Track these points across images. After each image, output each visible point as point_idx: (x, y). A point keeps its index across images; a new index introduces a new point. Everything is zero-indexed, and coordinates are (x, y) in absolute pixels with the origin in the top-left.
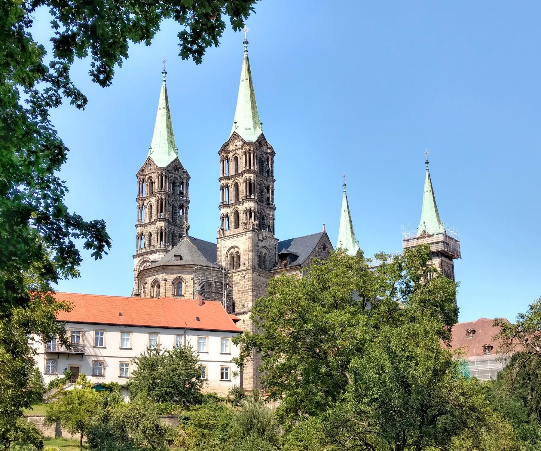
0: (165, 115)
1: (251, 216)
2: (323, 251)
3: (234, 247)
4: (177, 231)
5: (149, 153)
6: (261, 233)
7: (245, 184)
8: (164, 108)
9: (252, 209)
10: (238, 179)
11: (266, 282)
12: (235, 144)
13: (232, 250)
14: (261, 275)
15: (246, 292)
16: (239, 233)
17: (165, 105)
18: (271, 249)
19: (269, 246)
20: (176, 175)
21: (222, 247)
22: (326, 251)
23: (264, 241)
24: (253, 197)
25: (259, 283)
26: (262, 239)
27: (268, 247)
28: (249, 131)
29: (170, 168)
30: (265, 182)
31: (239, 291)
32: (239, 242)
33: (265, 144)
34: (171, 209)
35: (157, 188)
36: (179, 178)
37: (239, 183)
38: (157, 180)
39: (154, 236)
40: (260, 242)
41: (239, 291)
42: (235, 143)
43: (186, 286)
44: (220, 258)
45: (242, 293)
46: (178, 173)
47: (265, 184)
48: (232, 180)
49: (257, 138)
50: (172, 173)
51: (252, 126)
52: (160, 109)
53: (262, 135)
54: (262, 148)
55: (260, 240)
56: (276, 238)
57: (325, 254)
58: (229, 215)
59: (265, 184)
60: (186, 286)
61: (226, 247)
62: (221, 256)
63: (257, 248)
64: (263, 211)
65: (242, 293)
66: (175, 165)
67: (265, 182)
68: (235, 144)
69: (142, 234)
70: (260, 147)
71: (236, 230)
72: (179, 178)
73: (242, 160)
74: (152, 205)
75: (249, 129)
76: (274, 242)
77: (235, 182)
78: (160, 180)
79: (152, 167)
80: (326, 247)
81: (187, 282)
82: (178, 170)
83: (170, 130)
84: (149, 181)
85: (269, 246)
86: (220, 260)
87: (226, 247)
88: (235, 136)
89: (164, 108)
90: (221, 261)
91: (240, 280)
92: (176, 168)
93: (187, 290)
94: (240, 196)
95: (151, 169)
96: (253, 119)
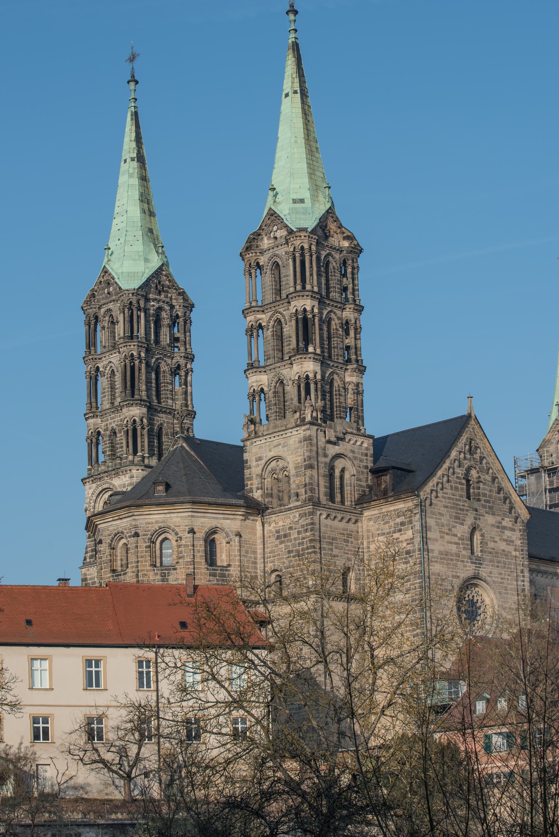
0: (136, 174)
1: (308, 392)
2: (468, 456)
3: (277, 458)
4: (168, 423)
5: (106, 260)
6: (330, 427)
7: (293, 323)
8: (133, 159)
9: (311, 375)
10: (281, 310)
11: (347, 530)
18: (356, 458)
19: (353, 452)
20: (161, 304)
21: (254, 459)
22: (477, 456)
24: (311, 349)
26: (333, 439)
31: (289, 552)
32: (286, 448)
35: (122, 335)
37: (283, 320)
38: (121, 318)
39: (121, 437)
40: (329, 446)
41: (289, 552)
42: (272, 233)
43: (179, 546)
44: (249, 483)
45: (294, 557)
49: (317, 221)
51: (306, 195)
52: (125, 161)
53: (330, 212)
55: (329, 442)
58: (266, 389)
60: (179, 546)
61: (260, 459)
62: (250, 479)
65: (294, 557)
69: (99, 433)
71: (279, 422)
74: (115, 370)
77: (275, 318)
78: (127, 319)
79: (111, 289)
81: (181, 538)
82: (167, 292)
83: (146, 206)
84: (107, 318)
85: (353, 452)
86: (249, 487)
87: (260, 459)
88: (273, 218)
89: (133, 159)
90: (251, 491)
91: (291, 528)
93: (181, 555)
94: (286, 349)
95: (109, 293)
96: (310, 178)
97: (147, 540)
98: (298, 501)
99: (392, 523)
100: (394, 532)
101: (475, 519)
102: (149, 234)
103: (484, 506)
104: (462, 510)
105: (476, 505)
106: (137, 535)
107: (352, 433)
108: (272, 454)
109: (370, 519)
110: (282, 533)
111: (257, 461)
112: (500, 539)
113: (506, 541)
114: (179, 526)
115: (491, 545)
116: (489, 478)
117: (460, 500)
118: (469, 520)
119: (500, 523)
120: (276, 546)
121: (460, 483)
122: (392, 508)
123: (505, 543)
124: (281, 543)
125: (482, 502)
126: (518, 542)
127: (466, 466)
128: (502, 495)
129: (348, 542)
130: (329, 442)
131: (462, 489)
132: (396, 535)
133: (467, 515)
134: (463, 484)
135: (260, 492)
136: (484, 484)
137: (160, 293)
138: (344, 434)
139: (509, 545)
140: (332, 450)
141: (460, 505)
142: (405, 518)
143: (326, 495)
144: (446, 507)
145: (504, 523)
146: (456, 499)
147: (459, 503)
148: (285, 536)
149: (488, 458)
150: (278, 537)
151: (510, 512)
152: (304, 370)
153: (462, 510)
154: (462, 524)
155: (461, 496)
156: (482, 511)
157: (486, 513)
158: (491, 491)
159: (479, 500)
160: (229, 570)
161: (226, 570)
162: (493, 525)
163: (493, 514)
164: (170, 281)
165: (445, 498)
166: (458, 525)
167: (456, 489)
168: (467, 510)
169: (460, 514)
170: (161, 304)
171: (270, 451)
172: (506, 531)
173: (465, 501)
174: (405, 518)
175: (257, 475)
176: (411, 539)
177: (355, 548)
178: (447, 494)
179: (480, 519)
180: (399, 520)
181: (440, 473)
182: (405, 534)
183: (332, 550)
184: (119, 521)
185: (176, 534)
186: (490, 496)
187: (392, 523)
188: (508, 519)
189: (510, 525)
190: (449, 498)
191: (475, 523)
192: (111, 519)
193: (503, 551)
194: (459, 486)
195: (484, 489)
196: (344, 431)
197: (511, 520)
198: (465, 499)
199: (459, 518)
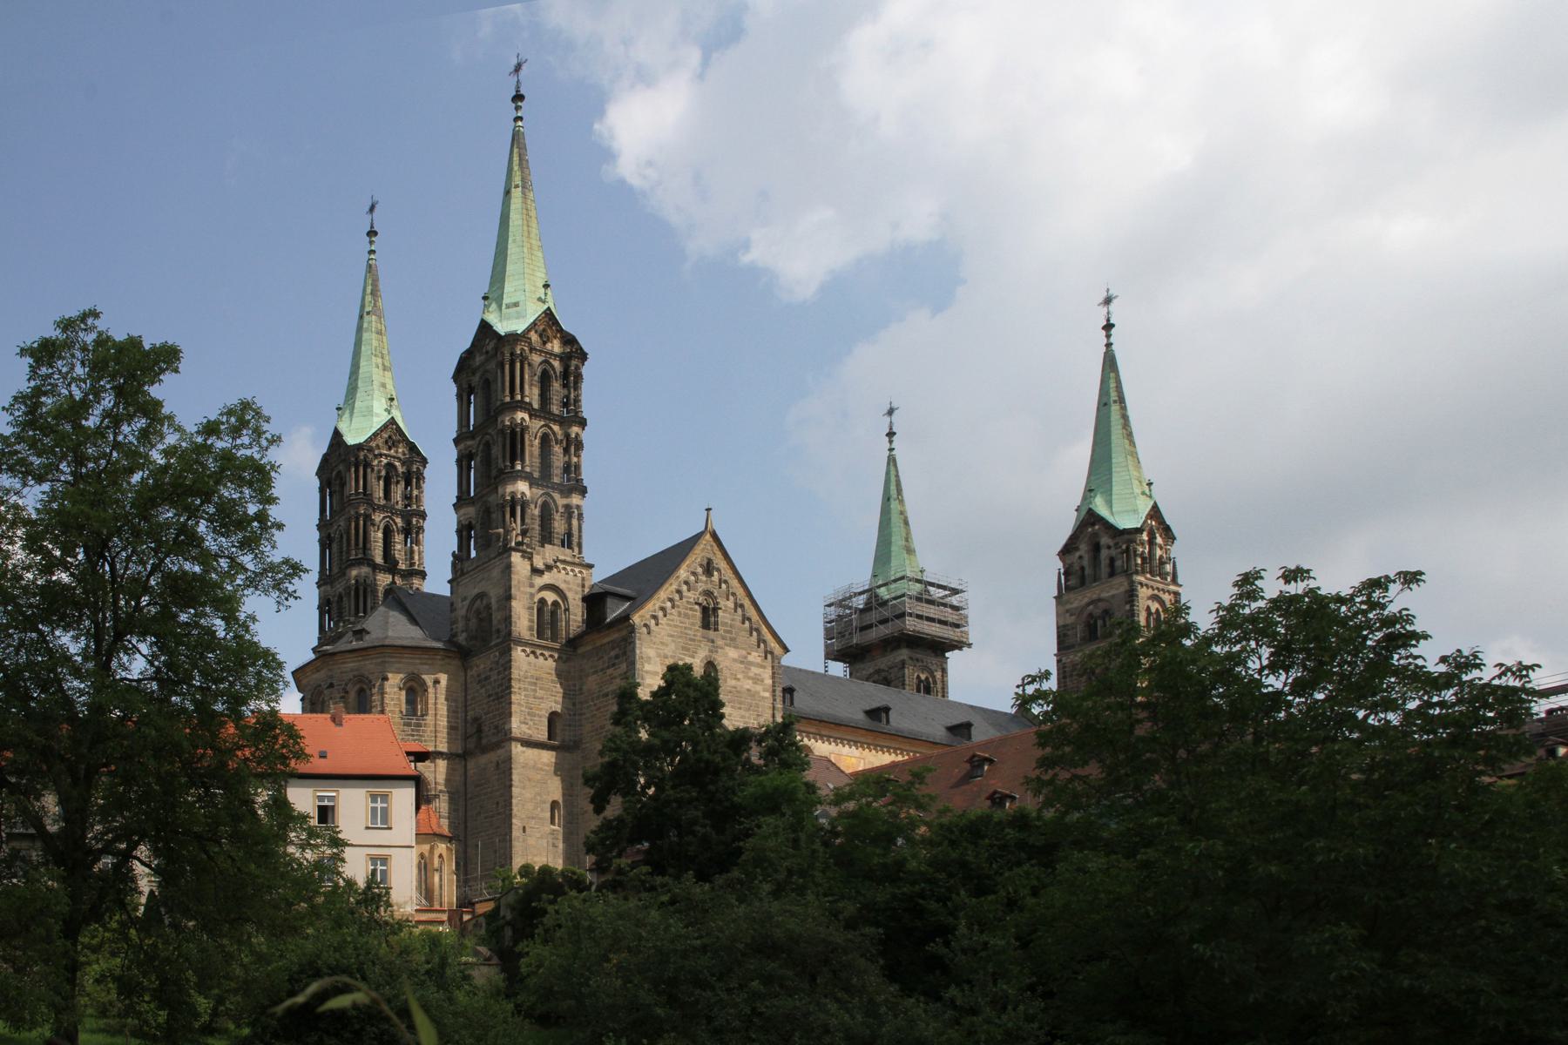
1: (513, 514)
6: (538, 554)
13: (479, 602)
15: (502, 697)
25: (533, 672)
27: (562, 586)
29: (373, 444)
31: (489, 696)
45: (494, 700)
46: (397, 452)
56: (588, 560)
57: (709, 587)
61: (464, 599)
64: (549, 499)
65: (494, 700)
66: (390, 437)
98: (498, 638)
99: (606, 658)
100: (608, 668)
101: (711, 651)
103: (724, 638)
104: (694, 640)
105: (711, 634)
108: (476, 591)
111: (462, 601)
112: (744, 677)
113: (753, 679)
117: (691, 629)
119: (746, 657)
120: (478, 691)
121: (691, 609)
122: (606, 640)
123: (750, 682)
124: (482, 687)
125: (721, 632)
131: (694, 616)
132: (610, 671)
134: (696, 611)
135: (464, 635)
136: (725, 611)
137: (390, 449)
139: (755, 683)
140: (540, 581)
143: (531, 629)
144: (672, 636)
145: (750, 658)
146: (685, 628)
147: (689, 632)
148: (487, 678)
150: (479, 682)
151: (759, 646)
153: (694, 640)
155: (693, 624)
156: (720, 642)
162: (735, 660)
167: (686, 616)
168: (700, 641)
179: (717, 652)
180: (613, 653)
181: (663, 594)
183: (535, 691)
187: (606, 658)
188: (756, 654)
189: (759, 660)
190: (676, 626)
193: (748, 690)
195: (724, 617)
199: (688, 650)
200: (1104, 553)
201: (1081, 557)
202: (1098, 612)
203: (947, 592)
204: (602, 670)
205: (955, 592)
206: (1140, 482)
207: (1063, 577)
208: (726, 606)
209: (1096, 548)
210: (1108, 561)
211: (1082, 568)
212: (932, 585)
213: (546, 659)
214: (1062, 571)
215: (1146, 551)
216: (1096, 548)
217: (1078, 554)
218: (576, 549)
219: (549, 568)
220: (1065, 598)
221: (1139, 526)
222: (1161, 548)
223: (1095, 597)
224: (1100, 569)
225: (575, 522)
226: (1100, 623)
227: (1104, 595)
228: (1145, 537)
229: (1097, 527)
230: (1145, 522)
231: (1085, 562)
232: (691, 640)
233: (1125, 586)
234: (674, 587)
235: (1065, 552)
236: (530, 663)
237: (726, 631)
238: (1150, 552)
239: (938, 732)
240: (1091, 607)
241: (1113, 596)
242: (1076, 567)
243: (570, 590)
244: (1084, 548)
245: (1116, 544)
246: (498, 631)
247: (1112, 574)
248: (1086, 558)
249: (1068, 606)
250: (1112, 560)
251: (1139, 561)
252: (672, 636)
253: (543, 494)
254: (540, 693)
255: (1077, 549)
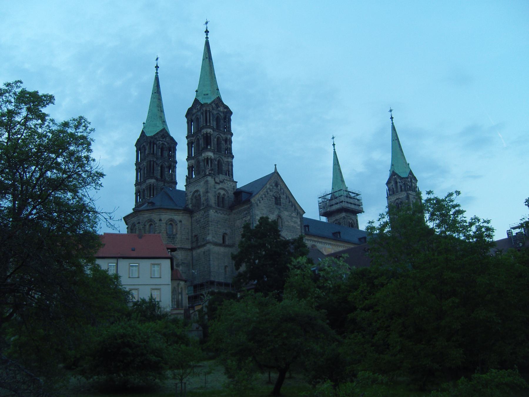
1: (208, 163)
2: (275, 188)
6: (217, 177)
12: (196, 108)
13: (196, 193)
14: (218, 212)
15: (205, 228)
16: (199, 178)
17: (157, 90)
19: (227, 187)
20: (163, 142)
21: (189, 192)
22: (279, 188)
23: (221, 184)
26: (218, 181)
27: (226, 189)
28: (207, 96)
29: (157, 137)
30: (222, 135)
31: (201, 227)
33: (222, 105)
34: (159, 168)
36: (166, 144)
37: (199, 138)
40: (216, 184)
45: (202, 229)
46: (166, 140)
47: (222, 137)
48: (195, 137)
50: (160, 141)
54: (219, 109)
55: (216, 183)
56: (235, 180)
59: (222, 137)
61: (190, 192)
63: (214, 190)
64: (221, 159)
65: (202, 229)
67: (222, 135)
68: (196, 108)
70: (217, 108)
72: (166, 144)
73: (201, 119)
75: (207, 94)
76: (233, 184)
80: (278, 184)
83: (159, 108)
85: (227, 187)
92: (163, 136)
97: (143, 225)
98: (203, 206)
99: (242, 214)
100: (244, 217)
101: (279, 212)
102: (160, 118)
103: (283, 208)
105: (279, 207)
106: (139, 223)
107: (227, 180)
108: (195, 189)
109: (235, 214)
110: (198, 220)
114: (156, 218)
115: (287, 223)
116: (285, 196)
117: (272, 205)
118: (276, 213)
119: (291, 215)
120: (196, 225)
121: (272, 198)
124: (198, 224)
125: (282, 206)
126: (299, 223)
127: (274, 191)
128: (291, 204)
129: (225, 223)
130: (216, 183)
132: (244, 219)
133: (275, 210)
135: (191, 205)
136: (283, 199)
137: (163, 139)
138: (224, 180)
139: (295, 223)
140: (218, 187)
141: (271, 206)
142: (247, 211)
143: (215, 203)
144: (265, 207)
145: (292, 215)
146: (270, 204)
147: (271, 206)
148: (199, 221)
149: (284, 189)
150: (197, 222)
151: (295, 211)
152: (206, 155)
154: (273, 214)
156: (282, 209)
157: (284, 210)
158: (286, 202)
159: (280, 205)
160: (176, 236)
161: (175, 236)
163: (287, 211)
164: (167, 134)
165: (264, 203)
166: (271, 214)
167: (270, 200)
168: (275, 209)
169: (272, 210)
170: (163, 142)
171: (194, 188)
172: (293, 218)
173: (274, 205)
174: (247, 211)
175: (190, 199)
176: (250, 219)
177: (229, 225)
178: (265, 202)
179: (281, 213)
180: (245, 213)
182: (247, 218)
183: (218, 225)
184: (134, 218)
185: (154, 221)
186: (285, 204)
188: (295, 214)
189: (295, 216)
190: (267, 204)
191: (279, 214)
192: (130, 218)
193: (293, 226)
194: (271, 199)
196: (223, 179)
197: (296, 214)
198: (274, 204)
200: (399, 184)
201: (392, 185)
202: (399, 202)
203: (355, 195)
204: (241, 218)
205: (358, 195)
206: (406, 164)
207: (388, 191)
208: (283, 197)
209: (396, 183)
210: (400, 187)
211: (393, 189)
212: (350, 192)
213: (221, 214)
214: (388, 189)
215: (410, 184)
216: (396, 183)
217: (391, 184)
218: (231, 176)
219: (221, 182)
220: (389, 198)
221: (407, 176)
222: (414, 184)
223: (398, 197)
224: (398, 189)
225: (230, 167)
226: (400, 205)
227: (400, 197)
228: (409, 180)
229: (396, 176)
230: (409, 175)
231: (394, 187)
232: (272, 208)
233: (405, 195)
234: (265, 190)
235: (388, 183)
236: (215, 216)
237: (283, 206)
238: (411, 184)
239: (356, 240)
240: (397, 201)
241: (403, 198)
242: (391, 188)
243: (229, 190)
244: (393, 183)
245: (401, 182)
246: (203, 204)
247: (401, 191)
248: (394, 185)
249: (391, 200)
250: (401, 187)
251: (408, 187)
252: (265, 207)
253: (218, 157)
254: (219, 226)
255: (391, 183)
